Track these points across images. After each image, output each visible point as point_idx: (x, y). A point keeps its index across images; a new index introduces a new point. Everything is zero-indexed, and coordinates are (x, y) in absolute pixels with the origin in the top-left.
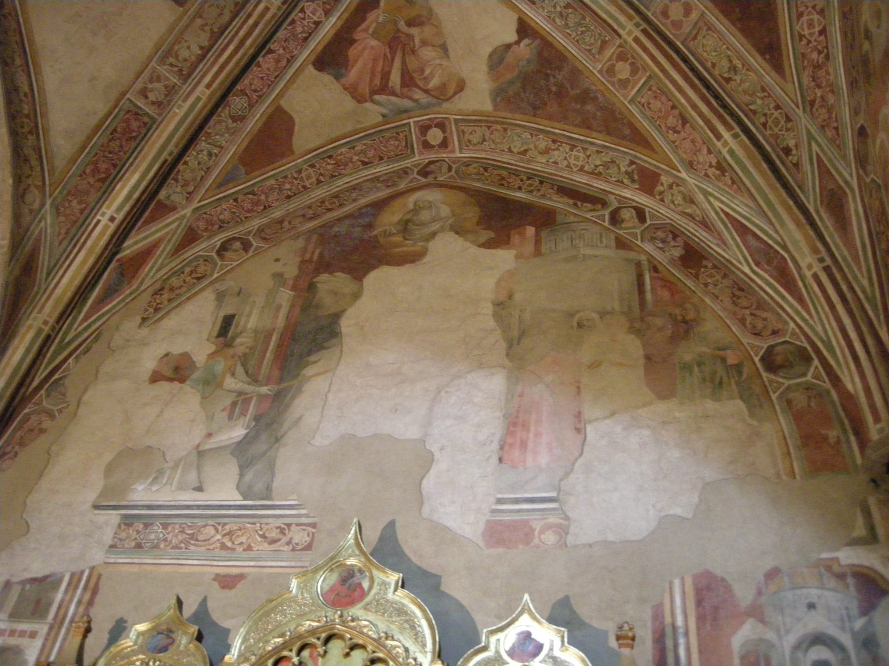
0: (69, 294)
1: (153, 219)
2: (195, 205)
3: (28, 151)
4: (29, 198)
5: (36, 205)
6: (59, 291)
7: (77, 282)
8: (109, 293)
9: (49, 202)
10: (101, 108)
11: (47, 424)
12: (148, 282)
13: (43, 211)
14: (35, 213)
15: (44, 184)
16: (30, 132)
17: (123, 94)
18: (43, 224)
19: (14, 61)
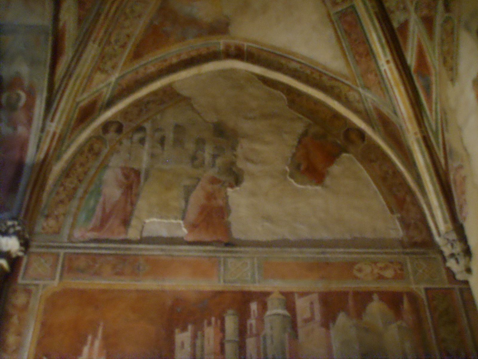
0: (411, 111)
1: (405, 38)
2: (412, 9)
3: (329, 83)
4: (351, 98)
5: (357, 97)
6: (405, 116)
7: (408, 103)
8: (428, 89)
9: (360, 90)
10: (329, 32)
11: (463, 172)
12: (437, 63)
13: (363, 95)
14: (361, 100)
15: (350, 86)
16: (321, 76)
17: (329, 15)
18: (368, 100)
19: (281, 64)
